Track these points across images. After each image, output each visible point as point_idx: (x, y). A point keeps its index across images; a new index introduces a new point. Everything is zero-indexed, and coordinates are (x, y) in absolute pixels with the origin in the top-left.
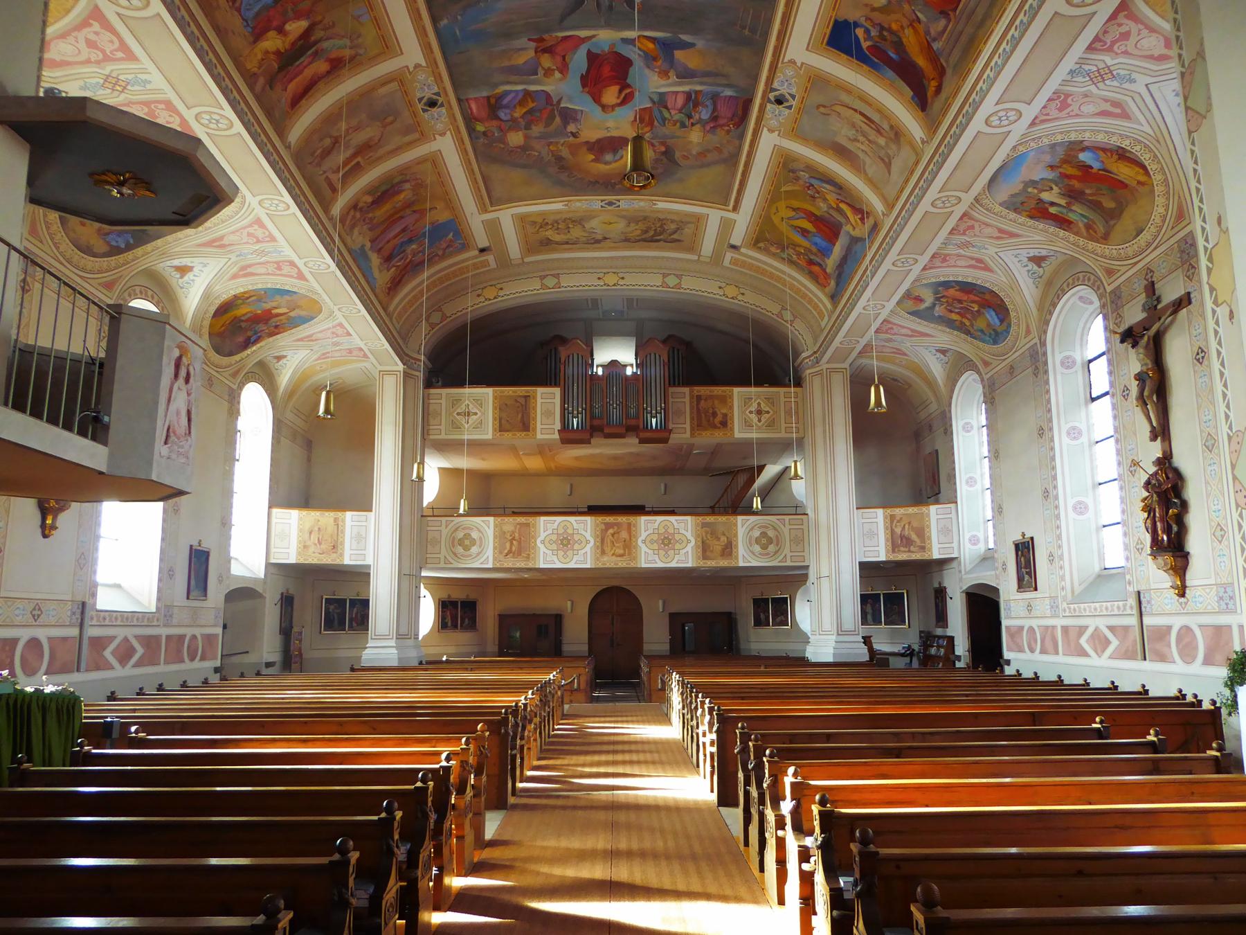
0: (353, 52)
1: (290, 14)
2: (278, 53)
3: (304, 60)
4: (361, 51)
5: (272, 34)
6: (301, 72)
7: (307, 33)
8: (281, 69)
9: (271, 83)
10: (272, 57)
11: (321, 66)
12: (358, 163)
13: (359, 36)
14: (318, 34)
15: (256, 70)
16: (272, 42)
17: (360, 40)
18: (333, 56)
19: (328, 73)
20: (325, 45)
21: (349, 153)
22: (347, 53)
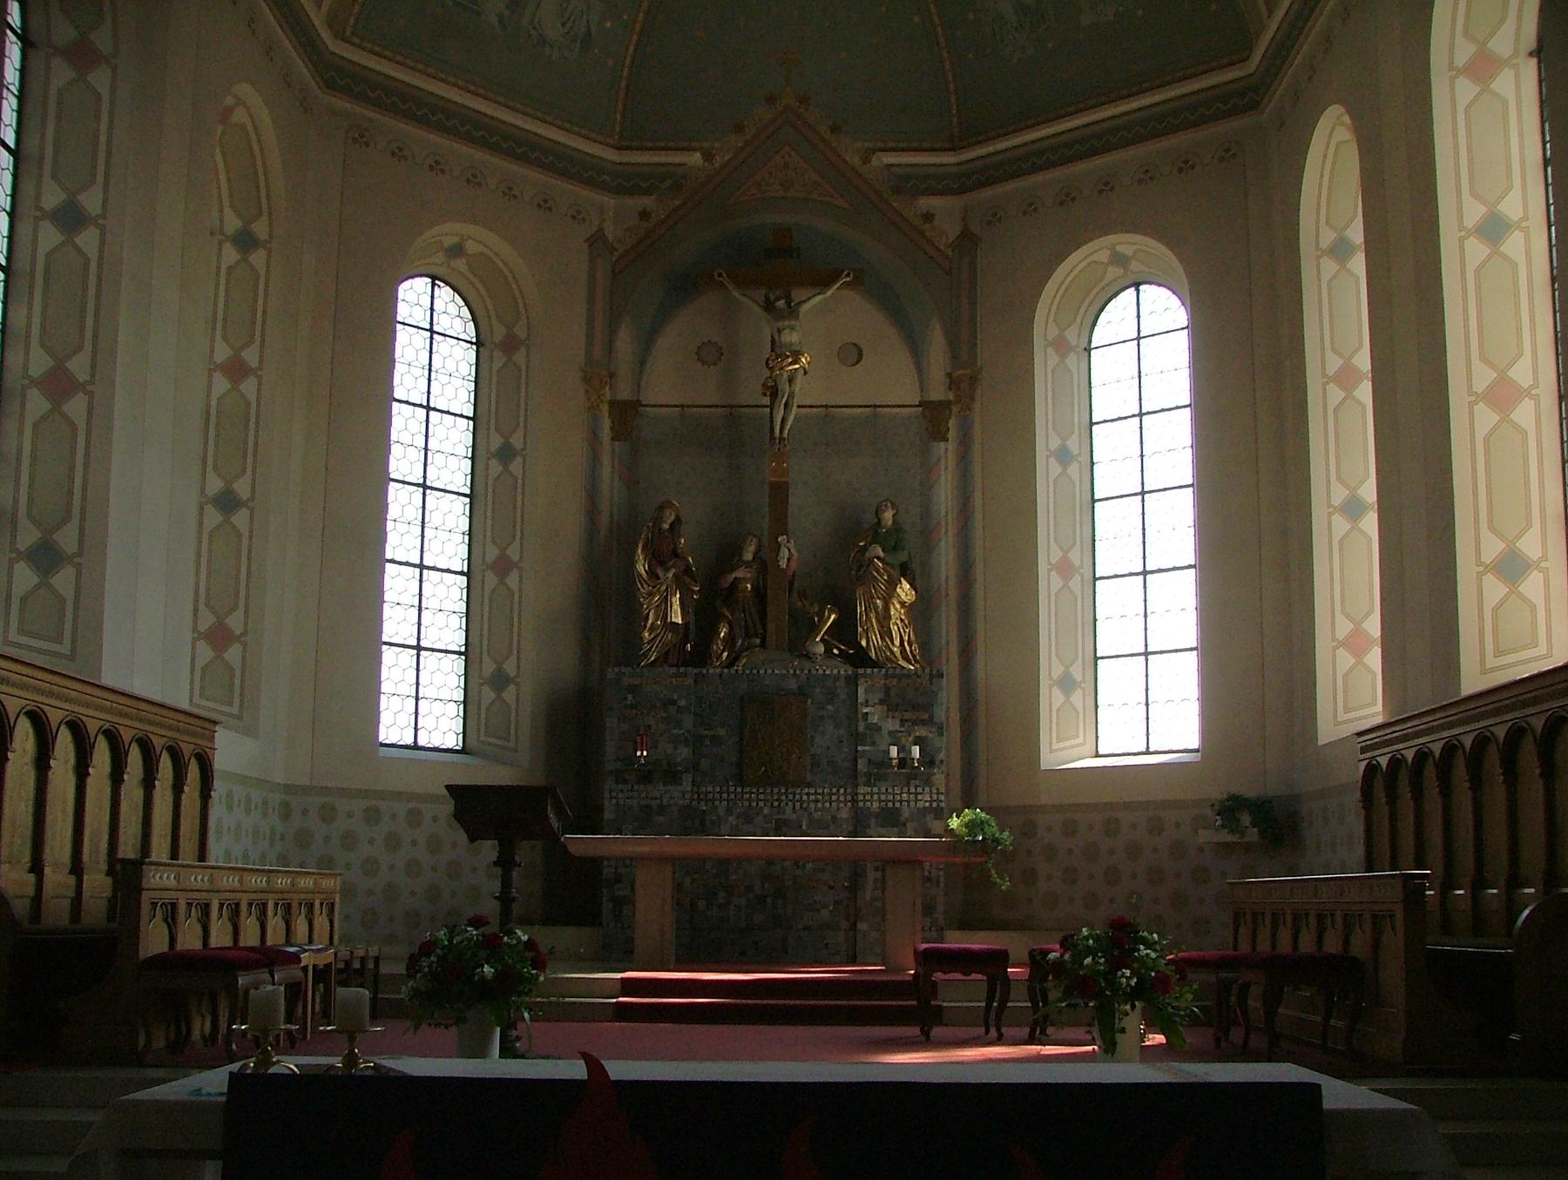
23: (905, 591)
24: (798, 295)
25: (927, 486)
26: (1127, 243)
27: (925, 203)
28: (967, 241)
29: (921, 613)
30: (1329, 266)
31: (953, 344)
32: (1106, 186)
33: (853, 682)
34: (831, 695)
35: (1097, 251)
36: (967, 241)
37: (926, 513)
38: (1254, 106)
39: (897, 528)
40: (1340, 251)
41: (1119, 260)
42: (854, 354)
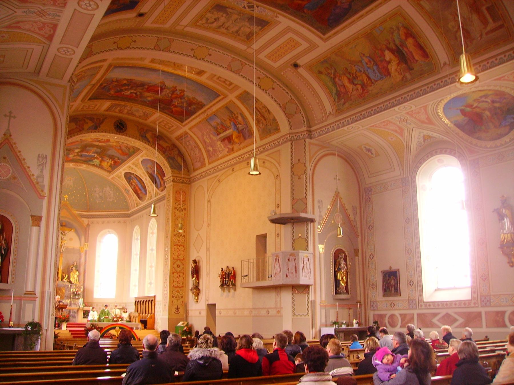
0: (402, 29)
1: (382, 58)
2: (398, 64)
3: (404, 50)
4: (400, 25)
5: (389, 67)
6: (411, 52)
7: (392, 51)
8: (406, 63)
9: (410, 69)
10: (399, 67)
11: (410, 41)
12: (488, 9)
13: (392, 28)
14: (392, 45)
15: (401, 77)
16: (393, 67)
17: (394, 27)
18: (403, 37)
19: (414, 38)
20: (397, 42)
21: (475, 17)
22: (402, 31)
23: (77, 273)
24: (66, 232)
25: (80, 259)
26: (110, 230)
27: (83, 219)
28: (88, 225)
29: (79, 276)
30: (136, 241)
31: (85, 239)
32: (109, 222)
33: (71, 286)
34: (68, 288)
35: (107, 230)
36: (88, 225)
37: (80, 262)
38: (129, 217)
39: (77, 265)
40: (137, 255)
41: (109, 231)
42: (71, 239)
